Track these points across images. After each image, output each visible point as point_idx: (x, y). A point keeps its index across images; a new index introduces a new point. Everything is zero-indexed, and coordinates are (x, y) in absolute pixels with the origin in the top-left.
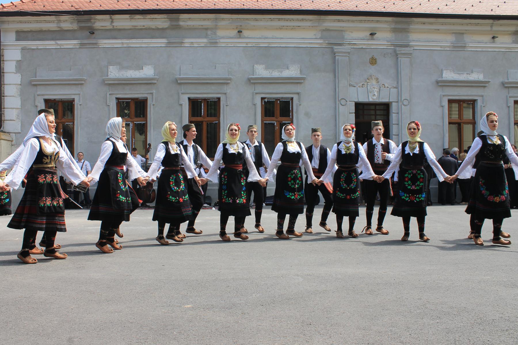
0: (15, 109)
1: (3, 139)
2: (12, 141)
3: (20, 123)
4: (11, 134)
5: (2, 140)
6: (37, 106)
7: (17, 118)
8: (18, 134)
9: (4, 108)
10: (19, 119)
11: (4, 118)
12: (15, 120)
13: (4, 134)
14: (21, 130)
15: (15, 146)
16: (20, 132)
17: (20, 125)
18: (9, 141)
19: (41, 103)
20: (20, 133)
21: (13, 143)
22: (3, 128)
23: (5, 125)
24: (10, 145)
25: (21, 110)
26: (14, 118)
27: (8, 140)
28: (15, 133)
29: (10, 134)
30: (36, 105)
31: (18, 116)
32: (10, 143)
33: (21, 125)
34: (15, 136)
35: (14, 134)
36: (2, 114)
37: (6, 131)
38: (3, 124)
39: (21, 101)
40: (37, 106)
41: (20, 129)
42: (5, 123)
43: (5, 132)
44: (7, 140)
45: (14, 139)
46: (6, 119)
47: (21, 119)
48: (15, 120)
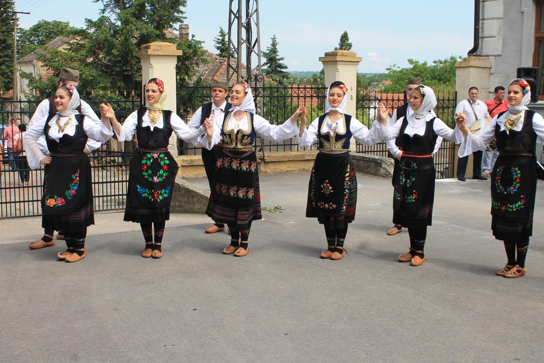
0: (496, 20)
1: (473, 65)
2: (490, 68)
3: (502, 40)
4: (490, 57)
5: (471, 68)
6: (523, 12)
7: (498, 33)
8: (499, 57)
9: (483, 19)
10: (500, 34)
11: (483, 35)
12: (495, 37)
13: (478, 59)
14: (502, 52)
15: (495, 75)
16: (501, 53)
17: (501, 43)
18: (485, 68)
19: (528, 8)
20: (500, 56)
21: (492, 71)
22: (482, 49)
23: (483, 44)
24: (488, 73)
25: (504, 20)
26: (494, 34)
27: (483, 66)
28: (495, 56)
29: (488, 58)
30: (522, 11)
31: (500, 29)
32: (485, 71)
33: (503, 42)
34: (495, 60)
35: (493, 58)
36: (480, 29)
37: (483, 54)
38: (482, 43)
39: (504, 6)
40: (523, 12)
41: (501, 50)
42: (484, 42)
43: (480, 56)
44: (480, 67)
45: (493, 65)
46: (486, 34)
47: (502, 34)
48: (495, 37)
